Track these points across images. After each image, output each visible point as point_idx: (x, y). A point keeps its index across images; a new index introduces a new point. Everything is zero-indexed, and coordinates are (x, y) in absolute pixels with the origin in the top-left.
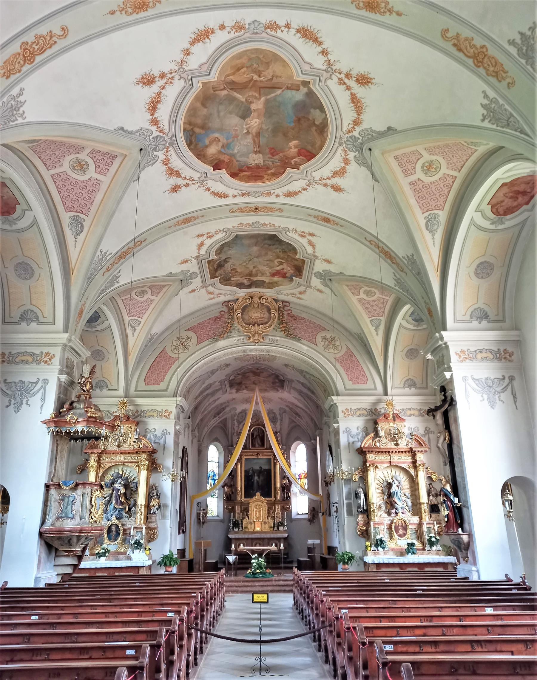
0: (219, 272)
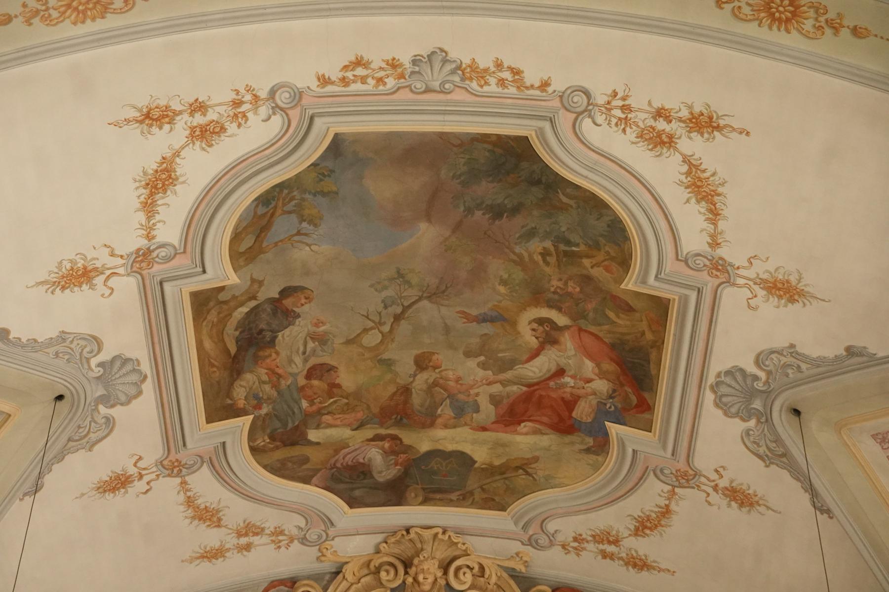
0: (249, 379)
